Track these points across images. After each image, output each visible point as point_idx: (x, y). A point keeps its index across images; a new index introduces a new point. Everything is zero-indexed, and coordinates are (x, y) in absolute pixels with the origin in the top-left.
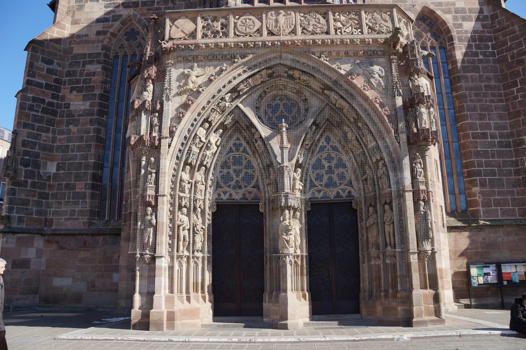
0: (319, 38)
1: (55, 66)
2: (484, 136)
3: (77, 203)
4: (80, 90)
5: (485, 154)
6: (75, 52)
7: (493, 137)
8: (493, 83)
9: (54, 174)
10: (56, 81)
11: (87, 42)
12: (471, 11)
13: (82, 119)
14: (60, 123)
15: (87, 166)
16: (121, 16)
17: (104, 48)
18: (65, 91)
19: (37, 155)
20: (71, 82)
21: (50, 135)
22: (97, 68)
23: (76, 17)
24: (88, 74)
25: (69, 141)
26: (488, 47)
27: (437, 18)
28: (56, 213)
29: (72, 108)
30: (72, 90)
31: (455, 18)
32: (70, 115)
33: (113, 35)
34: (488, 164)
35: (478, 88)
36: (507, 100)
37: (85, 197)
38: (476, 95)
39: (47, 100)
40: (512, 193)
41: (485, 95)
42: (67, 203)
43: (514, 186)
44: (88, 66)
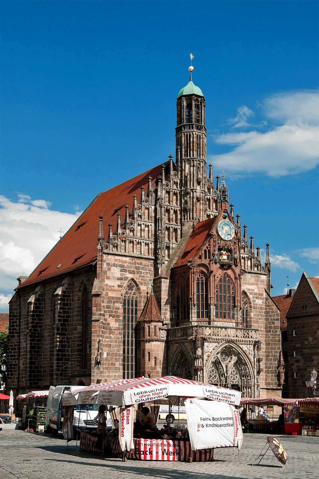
0: (240, 339)
3: (116, 372)
6: (109, 295)
8: (262, 329)
9: (106, 358)
11: (114, 290)
12: (259, 294)
14: (106, 332)
15: (120, 355)
16: (128, 278)
17: (122, 295)
18: (107, 316)
23: (108, 275)
24: (116, 309)
26: (262, 312)
27: (247, 296)
28: (108, 376)
29: (111, 325)
31: (253, 297)
32: (110, 329)
33: (125, 287)
36: (266, 337)
37: (119, 369)
42: (112, 372)
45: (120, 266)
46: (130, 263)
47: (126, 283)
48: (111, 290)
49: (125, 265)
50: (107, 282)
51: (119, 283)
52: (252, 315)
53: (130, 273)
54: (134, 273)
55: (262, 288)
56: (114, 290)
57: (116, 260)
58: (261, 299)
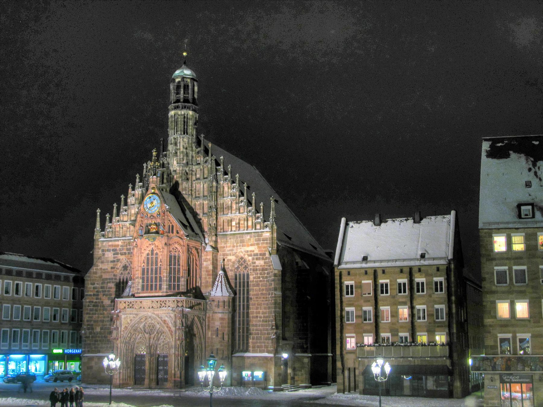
1: (96, 285)
2: (257, 317)
4: (106, 295)
5: (256, 325)
7: (260, 317)
8: (264, 292)
10: (97, 292)
12: (261, 254)
13: (108, 308)
14: (100, 310)
16: (119, 259)
18: (101, 296)
19: (92, 325)
20: (103, 291)
21: (97, 315)
22: (112, 285)
24: (110, 288)
25: (104, 318)
26: (265, 274)
29: (104, 303)
30: (104, 295)
31: (253, 259)
33: (118, 269)
34: (256, 330)
35: (257, 295)
38: (256, 298)
39: (95, 301)
40: (265, 343)
41: (260, 298)
42: (105, 344)
43: (266, 340)
44: (109, 284)
45: (113, 250)
46: (122, 246)
47: (120, 265)
48: (105, 273)
49: (118, 248)
50: (101, 266)
51: (111, 265)
52: (251, 278)
53: (122, 254)
54: (125, 254)
55: (264, 247)
56: (108, 272)
57: (110, 246)
58: (263, 259)
